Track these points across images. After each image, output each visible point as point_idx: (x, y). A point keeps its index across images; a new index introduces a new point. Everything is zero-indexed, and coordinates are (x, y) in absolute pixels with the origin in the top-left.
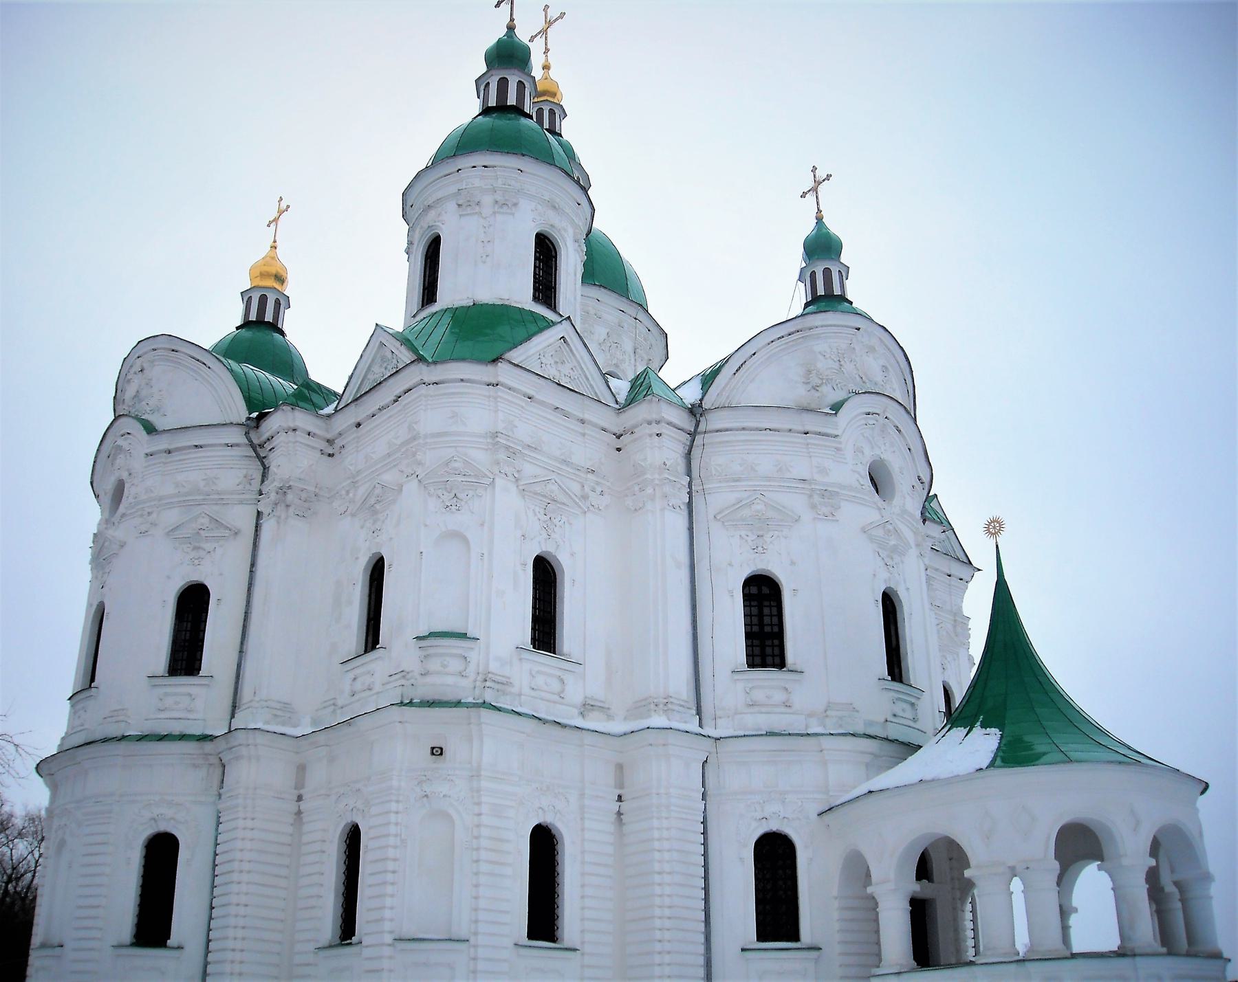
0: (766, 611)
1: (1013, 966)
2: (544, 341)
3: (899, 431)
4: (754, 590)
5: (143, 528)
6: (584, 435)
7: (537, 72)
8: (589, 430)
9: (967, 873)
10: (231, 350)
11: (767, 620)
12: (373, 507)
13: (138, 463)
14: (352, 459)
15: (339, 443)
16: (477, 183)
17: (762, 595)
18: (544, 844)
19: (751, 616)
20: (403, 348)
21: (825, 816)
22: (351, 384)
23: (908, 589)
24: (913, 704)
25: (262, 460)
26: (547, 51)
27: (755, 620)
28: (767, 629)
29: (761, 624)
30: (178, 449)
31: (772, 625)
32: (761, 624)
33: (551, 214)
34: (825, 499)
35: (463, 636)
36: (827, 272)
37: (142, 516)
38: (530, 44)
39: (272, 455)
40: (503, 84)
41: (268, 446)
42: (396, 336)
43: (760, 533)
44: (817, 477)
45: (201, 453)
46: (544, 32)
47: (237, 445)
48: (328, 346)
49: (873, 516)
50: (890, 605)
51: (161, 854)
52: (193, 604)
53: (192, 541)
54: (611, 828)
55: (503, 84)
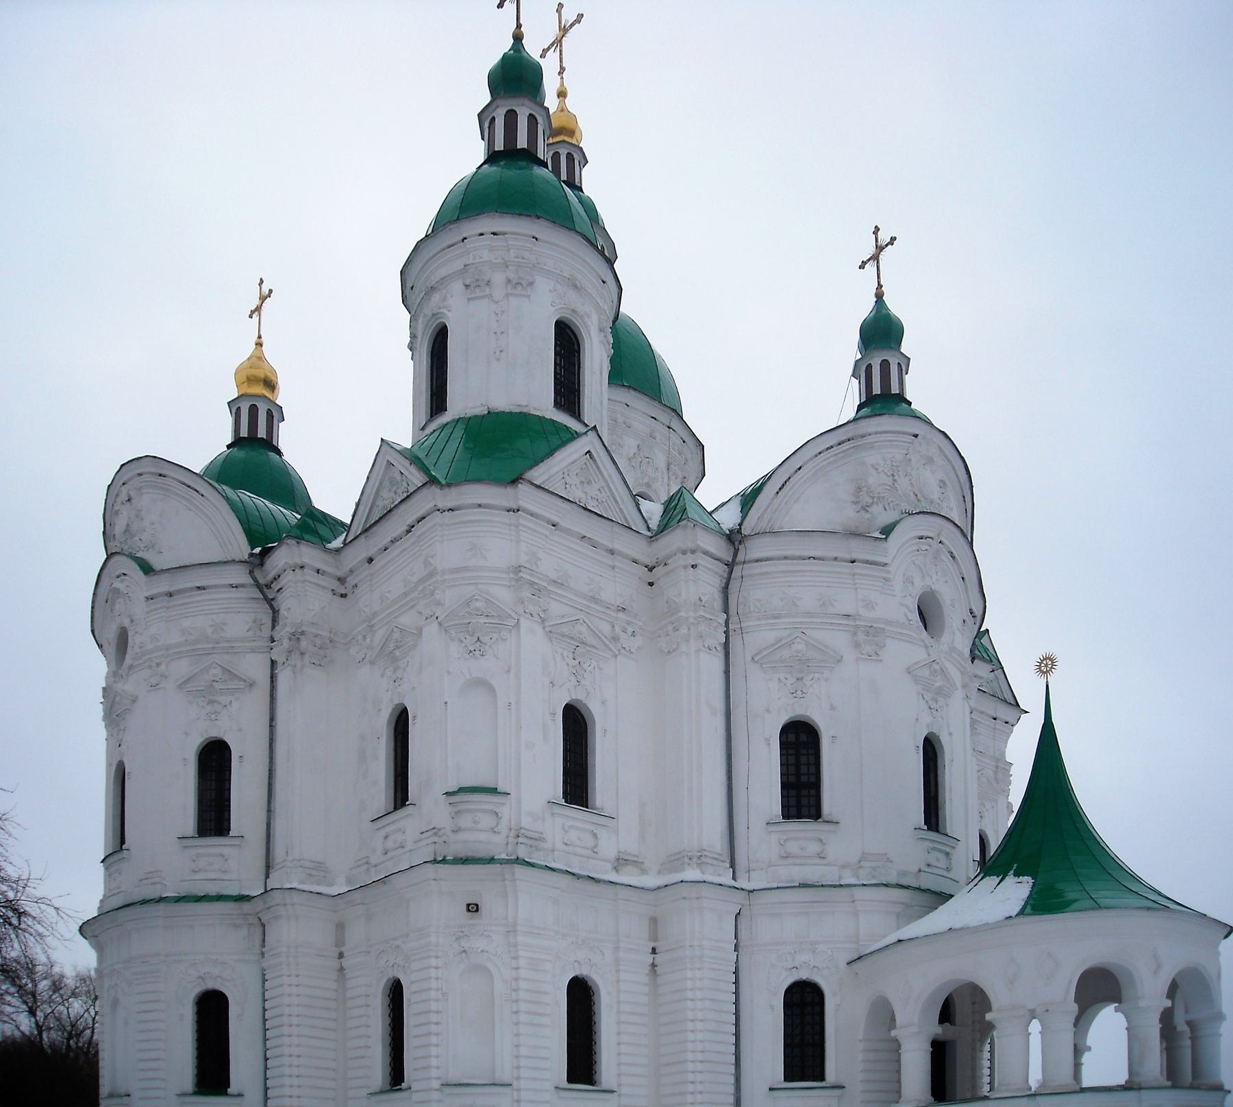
0: (803, 759)
1: (1025, 1099)
2: (571, 454)
3: (953, 557)
4: (792, 738)
5: (153, 681)
6: (613, 567)
7: (551, 102)
8: (619, 562)
9: (988, 1017)
10: (225, 473)
11: (804, 769)
12: (393, 653)
13: (139, 608)
14: (368, 600)
15: (351, 581)
16: (486, 255)
17: (800, 742)
19: (788, 765)
20: (413, 469)
21: (855, 966)
22: (359, 512)
23: (951, 734)
24: (947, 854)
25: (270, 602)
26: (562, 70)
27: (792, 769)
28: (804, 779)
29: (798, 774)
30: (179, 592)
31: (808, 774)
32: (798, 774)
33: (572, 294)
34: (869, 637)
35: (493, 791)
36: (885, 365)
37: (150, 667)
38: (542, 62)
39: (280, 597)
41: (275, 586)
42: (404, 453)
43: (800, 676)
44: (862, 612)
45: (203, 596)
46: (558, 42)
47: (243, 586)
48: (332, 464)
49: (919, 655)
50: (931, 751)
51: (212, 1011)
52: (214, 761)
53: (207, 693)
54: (646, 979)
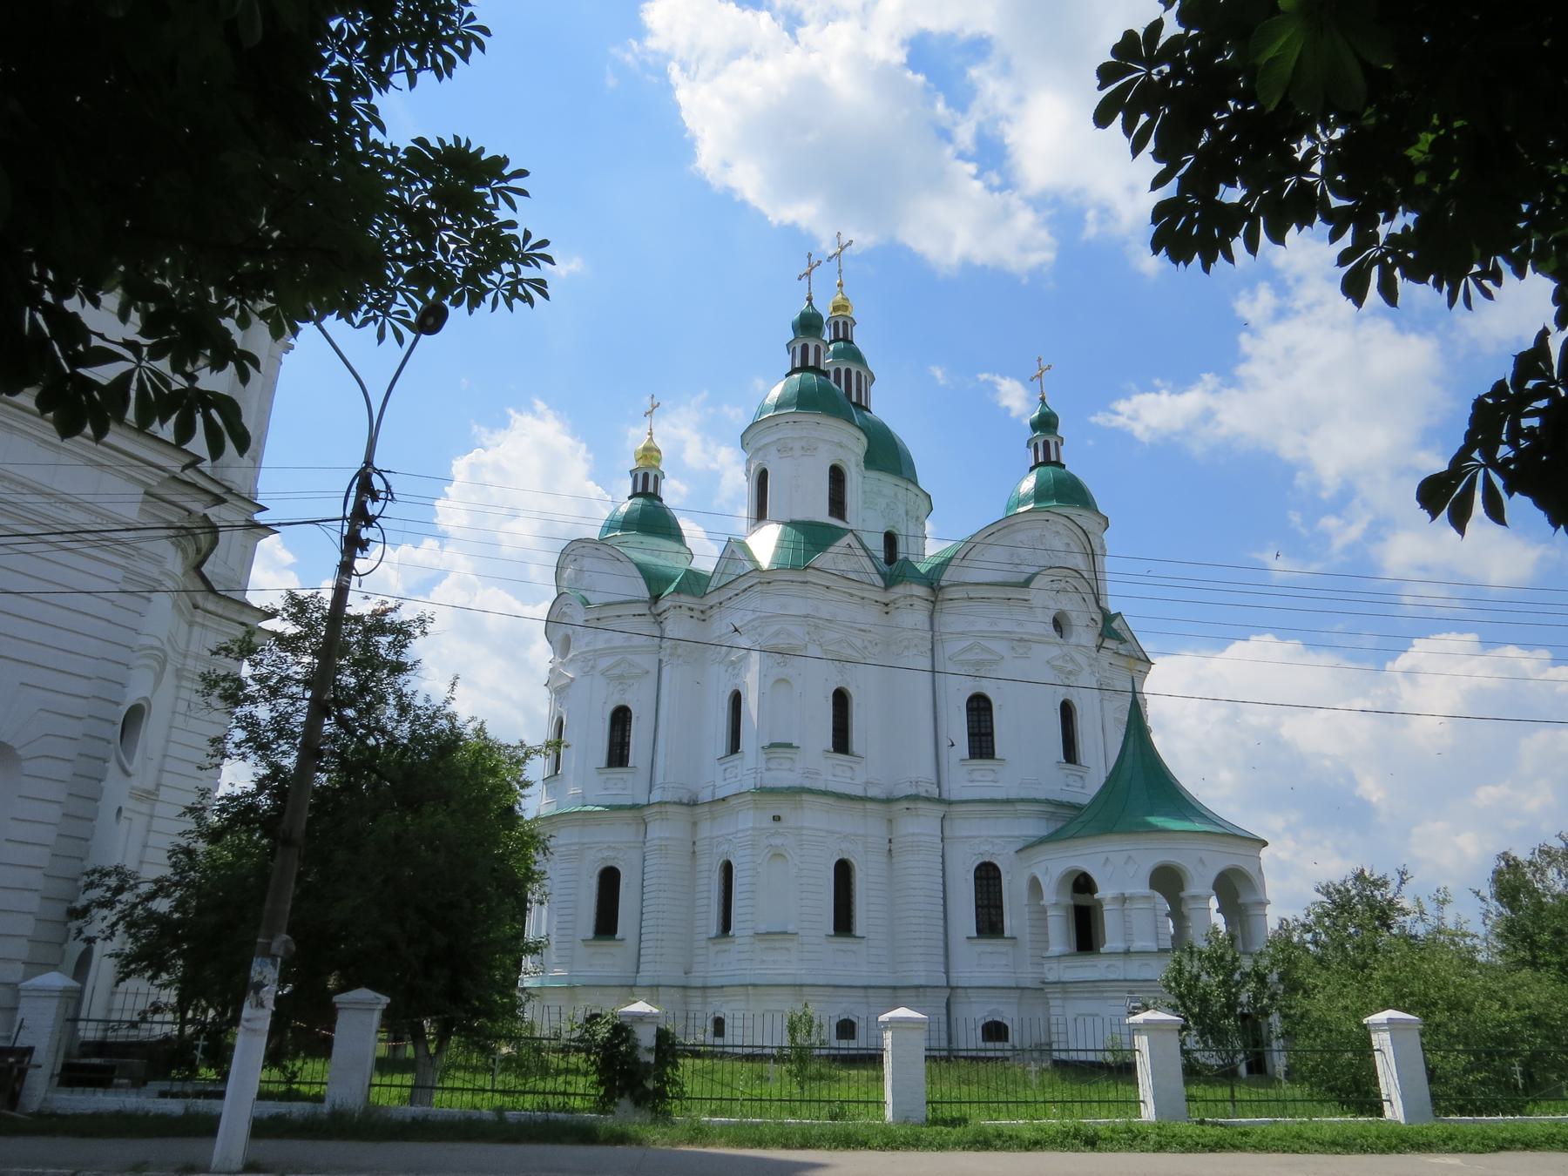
15: (709, 613)
17: (979, 708)
18: (843, 872)
35: (789, 746)
40: (805, 348)
55: (805, 348)
